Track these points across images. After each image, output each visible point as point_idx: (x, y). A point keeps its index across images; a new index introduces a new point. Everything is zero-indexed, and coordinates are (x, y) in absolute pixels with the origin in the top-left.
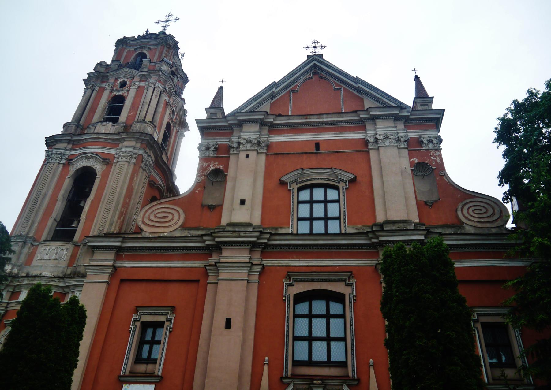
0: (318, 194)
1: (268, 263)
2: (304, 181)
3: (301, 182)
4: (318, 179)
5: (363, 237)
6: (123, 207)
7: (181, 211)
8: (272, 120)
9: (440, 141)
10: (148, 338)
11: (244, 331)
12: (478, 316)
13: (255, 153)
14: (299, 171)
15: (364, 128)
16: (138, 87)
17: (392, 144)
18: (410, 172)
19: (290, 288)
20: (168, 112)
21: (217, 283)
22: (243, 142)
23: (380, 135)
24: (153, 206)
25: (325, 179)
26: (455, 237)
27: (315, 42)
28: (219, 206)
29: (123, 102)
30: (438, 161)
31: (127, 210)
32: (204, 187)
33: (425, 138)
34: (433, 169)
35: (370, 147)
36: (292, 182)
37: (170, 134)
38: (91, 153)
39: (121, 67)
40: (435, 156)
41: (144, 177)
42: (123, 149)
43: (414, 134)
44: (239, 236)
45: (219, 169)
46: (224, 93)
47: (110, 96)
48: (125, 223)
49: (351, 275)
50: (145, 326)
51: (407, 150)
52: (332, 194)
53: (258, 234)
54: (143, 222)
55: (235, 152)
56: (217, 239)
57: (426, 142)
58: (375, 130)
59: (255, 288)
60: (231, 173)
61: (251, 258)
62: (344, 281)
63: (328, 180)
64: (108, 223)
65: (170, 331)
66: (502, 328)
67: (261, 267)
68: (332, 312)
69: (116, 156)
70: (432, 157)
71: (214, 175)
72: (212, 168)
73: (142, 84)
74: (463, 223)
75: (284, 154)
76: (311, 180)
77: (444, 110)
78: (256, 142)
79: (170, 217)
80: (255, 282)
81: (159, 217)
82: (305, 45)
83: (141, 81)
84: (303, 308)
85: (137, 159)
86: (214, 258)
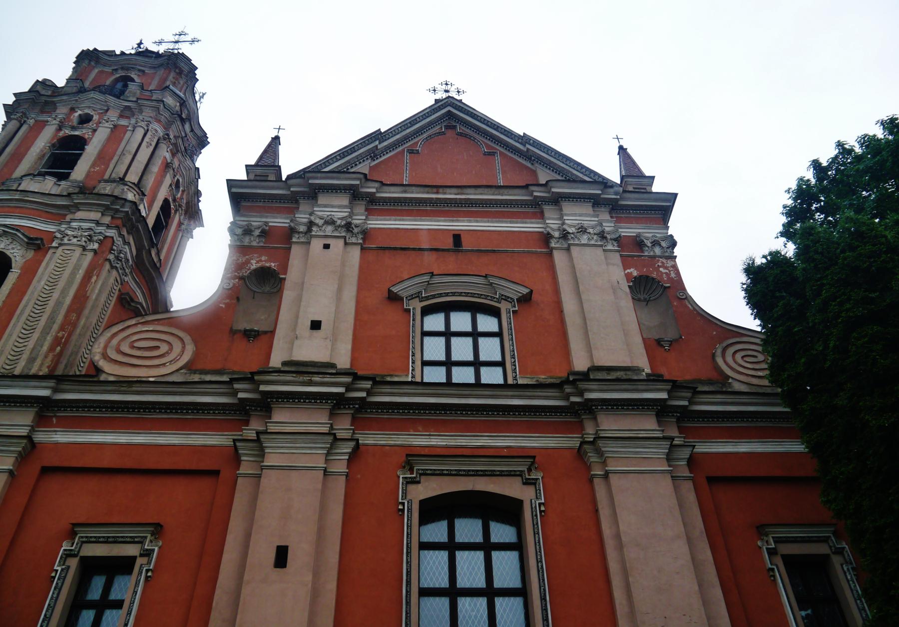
0: (461, 321)
1: (369, 439)
2: (434, 297)
3: (427, 298)
4: (460, 294)
6: (62, 328)
7: (187, 339)
8: (374, 190)
9: (674, 244)
10: (95, 593)
11: (316, 574)
12: (775, 542)
13: (341, 242)
14: (426, 278)
15: (541, 216)
16: (115, 126)
17: (593, 242)
18: (628, 290)
19: (411, 487)
20: (168, 180)
21: (259, 476)
22: (320, 222)
23: (570, 226)
24: (129, 327)
25: (473, 295)
26: (719, 398)
27: (447, 84)
28: (266, 333)
29: (83, 149)
30: (673, 275)
31: (70, 335)
32: (238, 299)
33: (647, 239)
34: (665, 288)
35: (553, 245)
36: (411, 297)
37: (167, 223)
39: (82, 90)
40: (666, 268)
41: (112, 280)
42: (74, 224)
43: (629, 231)
44: (310, 383)
45: (269, 268)
46: (281, 148)
47: (55, 136)
48: (64, 361)
49: (533, 463)
50: (90, 567)
51: (617, 255)
52: (486, 323)
53: (348, 380)
54: (105, 356)
55: (302, 240)
56: (263, 388)
57: (649, 245)
58: (561, 218)
59: (339, 486)
60: (292, 276)
61: (332, 428)
62: (520, 475)
63: (480, 296)
64: (25, 356)
65: (147, 577)
66: (821, 564)
67: (352, 444)
68: (494, 539)
69: (59, 235)
70: (661, 269)
71: (258, 278)
72: (254, 265)
73: (123, 122)
74: (728, 377)
75: (395, 249)
76: (447, 295)
77: (676, 195)
78: (343, 223)
79: (164, 348)
80: (339, 474)
81: (139, 348)
82: (431, 87)
83: (121, 116)
84: (437, 531)
85: (101, 243)
86: (256, 425)
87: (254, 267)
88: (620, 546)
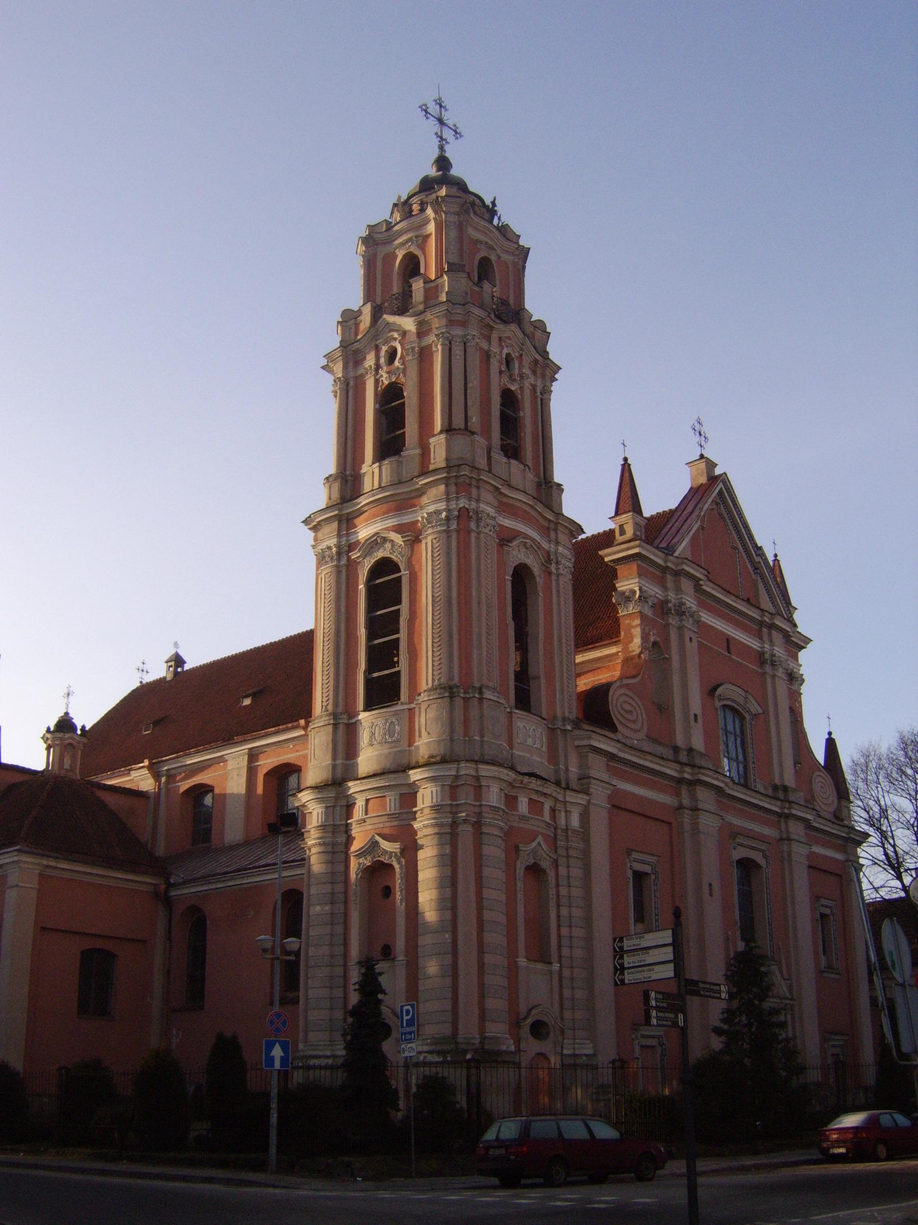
5: (779, 803)
38: (533, 540)
87: (652, 639)
88: (793, 903)
